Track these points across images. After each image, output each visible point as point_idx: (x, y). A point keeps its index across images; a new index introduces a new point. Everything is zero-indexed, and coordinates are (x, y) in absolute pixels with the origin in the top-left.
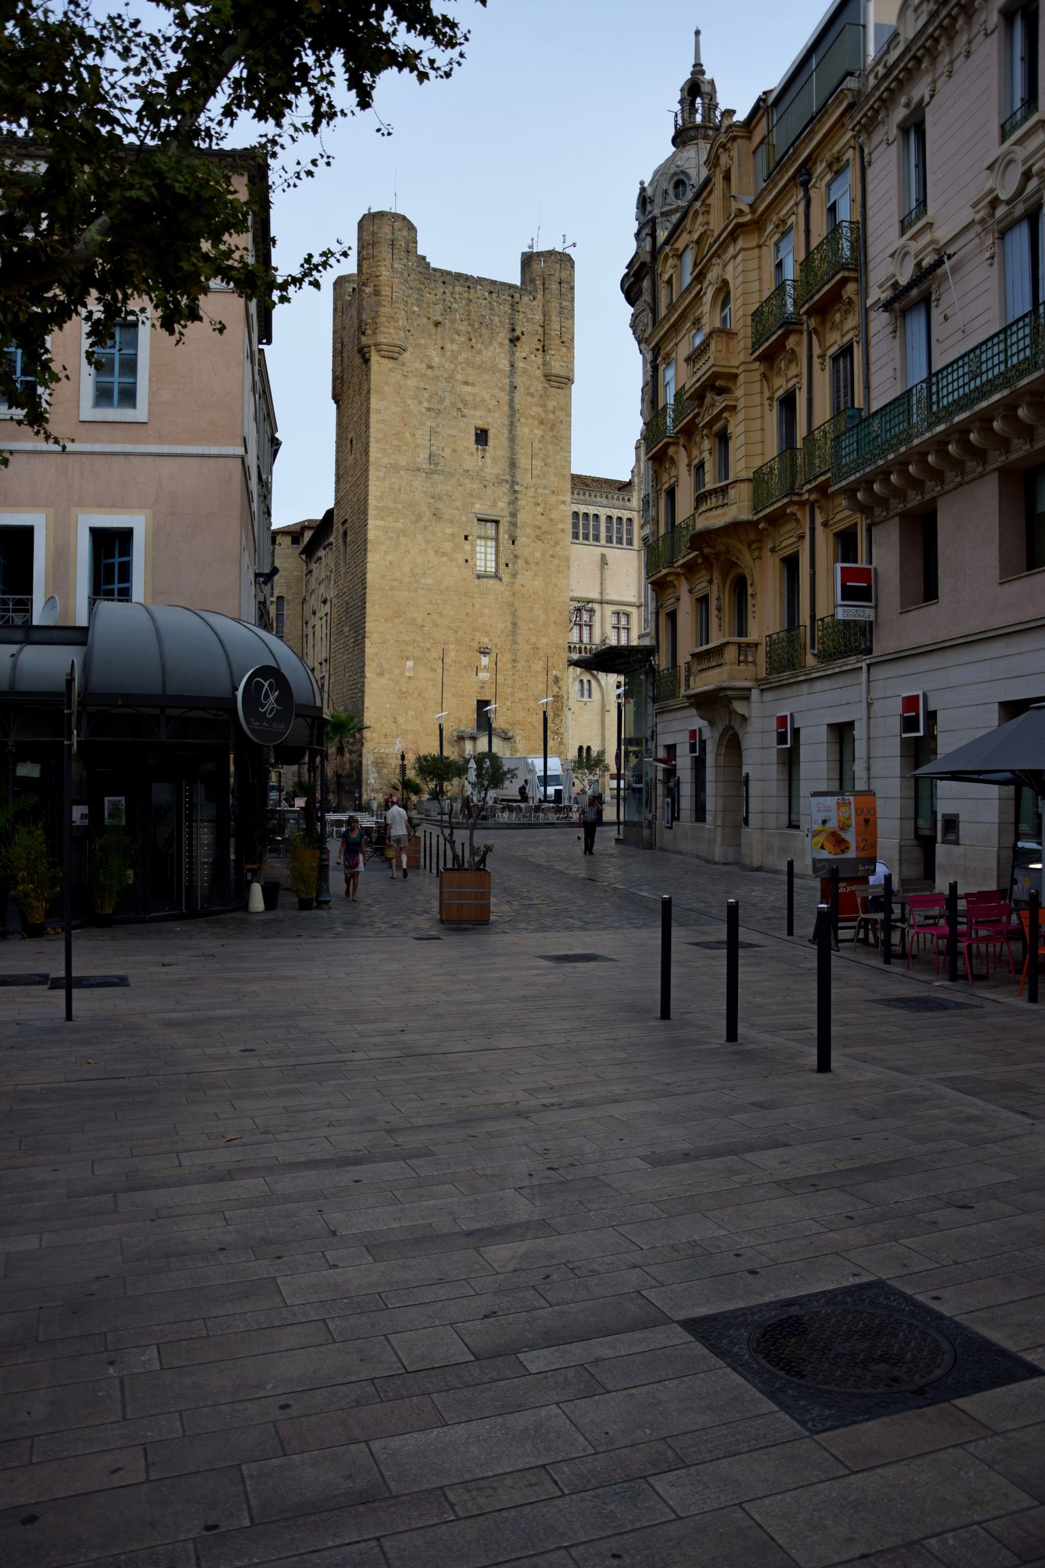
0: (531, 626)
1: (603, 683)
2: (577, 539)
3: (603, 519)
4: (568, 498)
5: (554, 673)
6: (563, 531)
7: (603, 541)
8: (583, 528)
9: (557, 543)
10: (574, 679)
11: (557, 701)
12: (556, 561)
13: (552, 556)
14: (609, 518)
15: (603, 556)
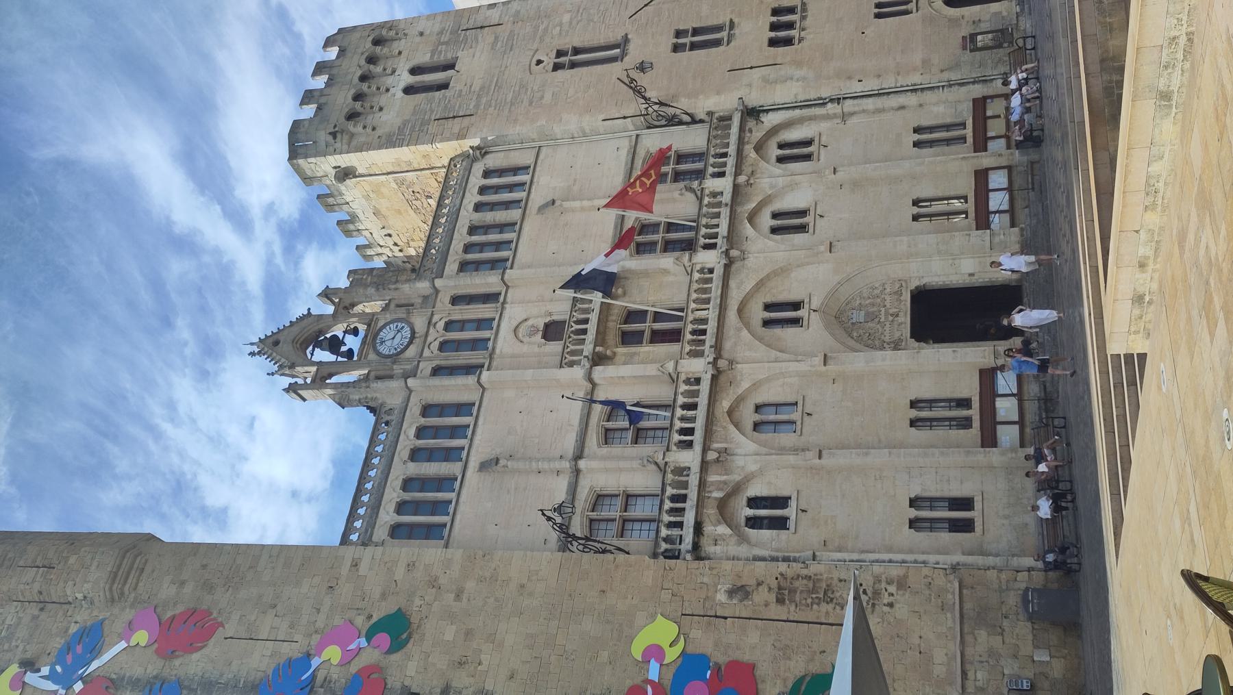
0: (606, 654)
1: (752, 467)
2: (445, 525)
3: (414, 469)
4: (349, 553)
5: (721, 597)
6: (410, 566)
7: (453, 468)
8: (424, 513)
9: (433, 583)
10: (743, 539)
11: (792, 591)
12: (470, 585)
13: (458, 597)
14: (415, 455)
15: (484, 466)
